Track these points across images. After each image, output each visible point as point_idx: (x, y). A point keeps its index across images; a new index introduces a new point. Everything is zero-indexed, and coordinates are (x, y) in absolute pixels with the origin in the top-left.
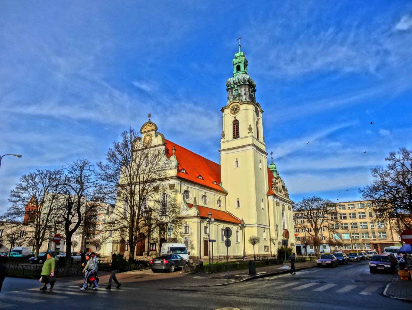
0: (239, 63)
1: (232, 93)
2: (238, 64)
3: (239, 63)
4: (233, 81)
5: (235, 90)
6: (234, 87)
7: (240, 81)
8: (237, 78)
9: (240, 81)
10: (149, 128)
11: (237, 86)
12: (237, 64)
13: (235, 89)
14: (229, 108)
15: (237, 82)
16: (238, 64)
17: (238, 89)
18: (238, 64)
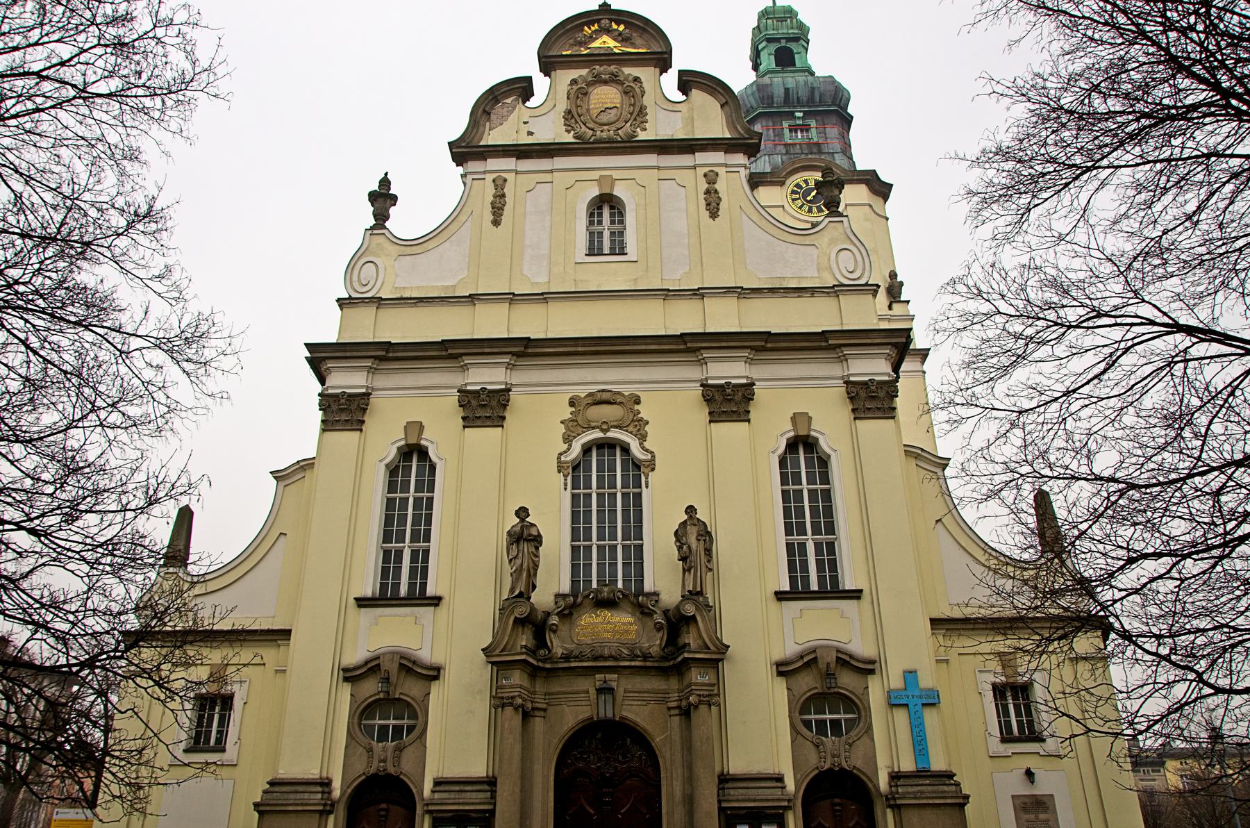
0: (789, 40)
1: (780, 135)
2: (783, 42)
3: (789, 40)
4: (787, 90)
5: (793, 129)
6: (793, 113)
7: (817, 98)
8: (806, 83)
9: (817, 98)
10: (606, 42)
11: (805, 112)
12: (777, 40)
13: (792, 123)
14: (782, 184)
15: (805, 99)
16: (783, 42)
17: (805, 129)
18: (783, 43)
